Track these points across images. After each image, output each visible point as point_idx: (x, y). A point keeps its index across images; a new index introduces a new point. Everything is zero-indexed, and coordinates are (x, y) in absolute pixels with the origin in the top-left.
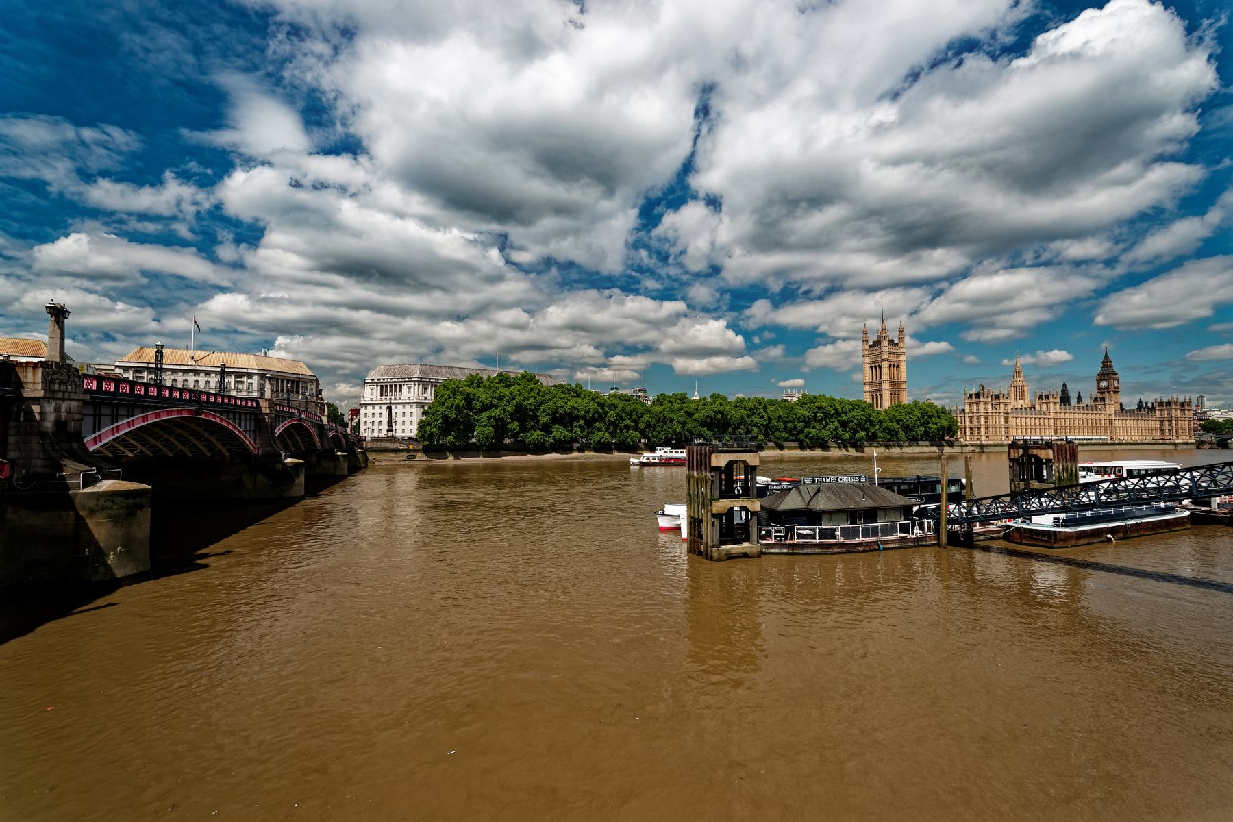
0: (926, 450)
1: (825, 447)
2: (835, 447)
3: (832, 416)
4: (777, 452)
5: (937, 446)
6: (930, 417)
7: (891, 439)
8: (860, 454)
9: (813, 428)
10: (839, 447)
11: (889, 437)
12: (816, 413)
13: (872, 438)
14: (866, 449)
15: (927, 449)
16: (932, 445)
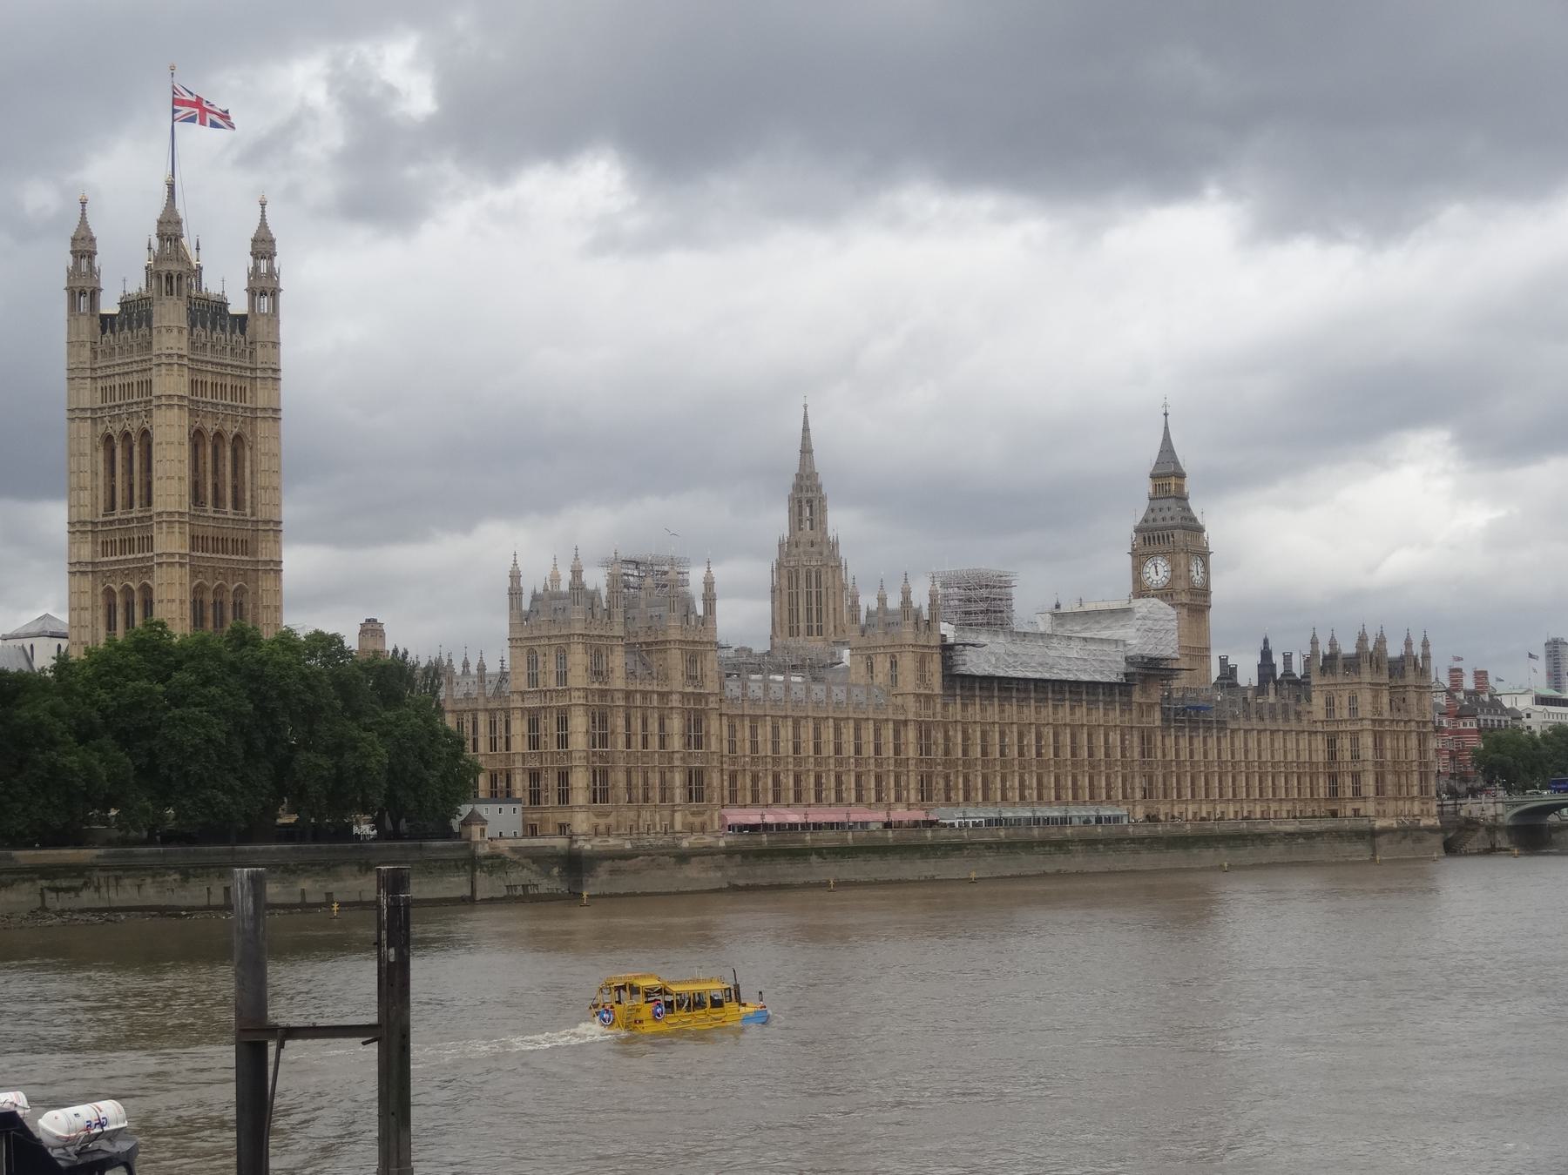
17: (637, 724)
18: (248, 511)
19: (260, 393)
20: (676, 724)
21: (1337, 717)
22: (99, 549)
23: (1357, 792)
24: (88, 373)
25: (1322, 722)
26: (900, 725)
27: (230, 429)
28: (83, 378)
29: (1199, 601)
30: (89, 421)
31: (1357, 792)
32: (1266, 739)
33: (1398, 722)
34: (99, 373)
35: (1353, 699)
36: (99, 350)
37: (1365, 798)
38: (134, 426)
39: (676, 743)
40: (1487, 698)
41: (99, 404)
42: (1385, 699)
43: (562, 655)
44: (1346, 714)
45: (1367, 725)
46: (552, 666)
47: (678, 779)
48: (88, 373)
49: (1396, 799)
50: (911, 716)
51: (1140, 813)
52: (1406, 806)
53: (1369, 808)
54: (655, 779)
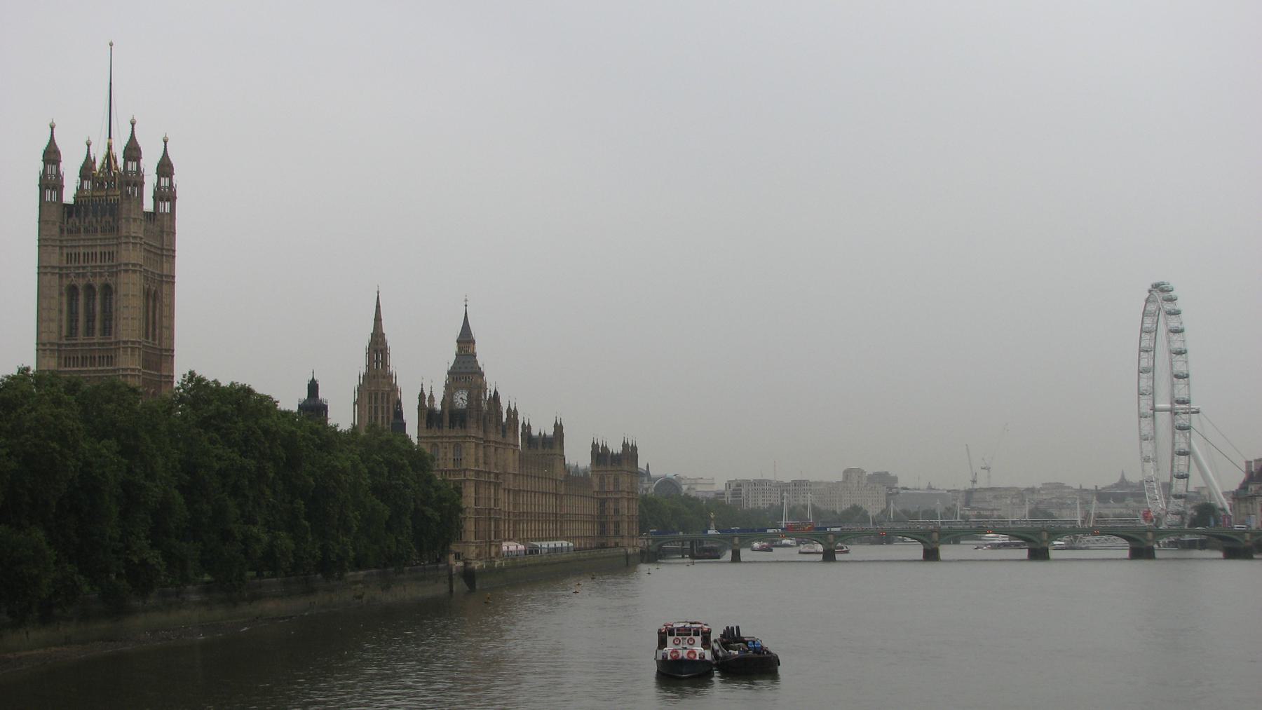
18: (157, 342)
19: (165, 265)
21: (606, 489)
22: (63, 362)
23: (617, 532)
24: (58, 243)
25: (597, 492)
28: (53, 246)
30: (58, 275)
31: (617, 532)
34: (65, 243)
35: (616, 480)
36: (65, 228)
37: (623, 536)
38: (98, 283)
41: (64, 264)
43: (458, 447)
44: (612, 489)
45: (625, 495)
46: (450, 455)
48: (58, 243)
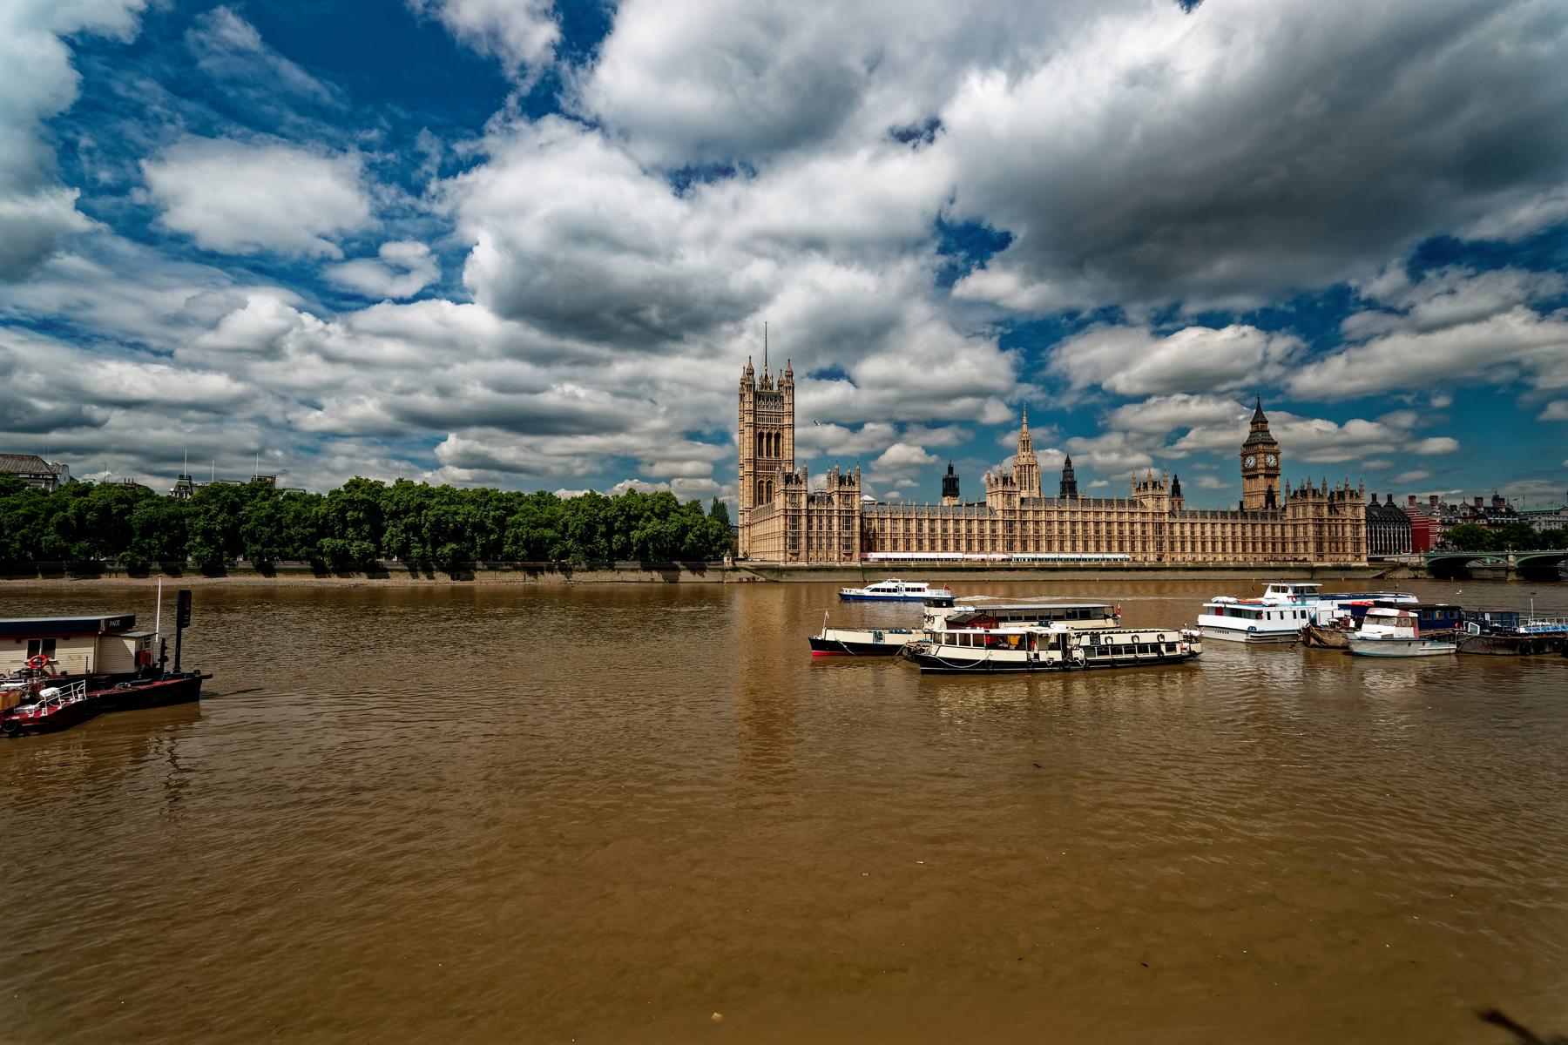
0: (631, 576)
1: (377, 571)
2: (401, 571)
3: (395, 515)
4: (259, 580)
5: (658, 570)
6: (637, 518)
7: (536, 556)
8: (458, 583)
9: (342, 536)
10: (413, 572)
11: (524, 552)
12: (343, 511)
13: (494, 557)
14: (477, 575)
15: (631, 577)
16: (646, 569)
17: (815, 521)
20: (835, 521)
23: (1306, 549)
26: (994, 522)
27: (774, 432)
29: (1271, 472)
31: (1306, 549)
32: (1249, 528)
33: (1336, 520)
39: (835, 529)
40: (1504, 510)
42: (1326, 509)
45: (1311, 521)
47: (836, 541)
49: (1330, 552)
50: (1000, 518)
51: (1152, 558)
52: (1342, 558)
53: (1310, 558)
54: (824, 541)
